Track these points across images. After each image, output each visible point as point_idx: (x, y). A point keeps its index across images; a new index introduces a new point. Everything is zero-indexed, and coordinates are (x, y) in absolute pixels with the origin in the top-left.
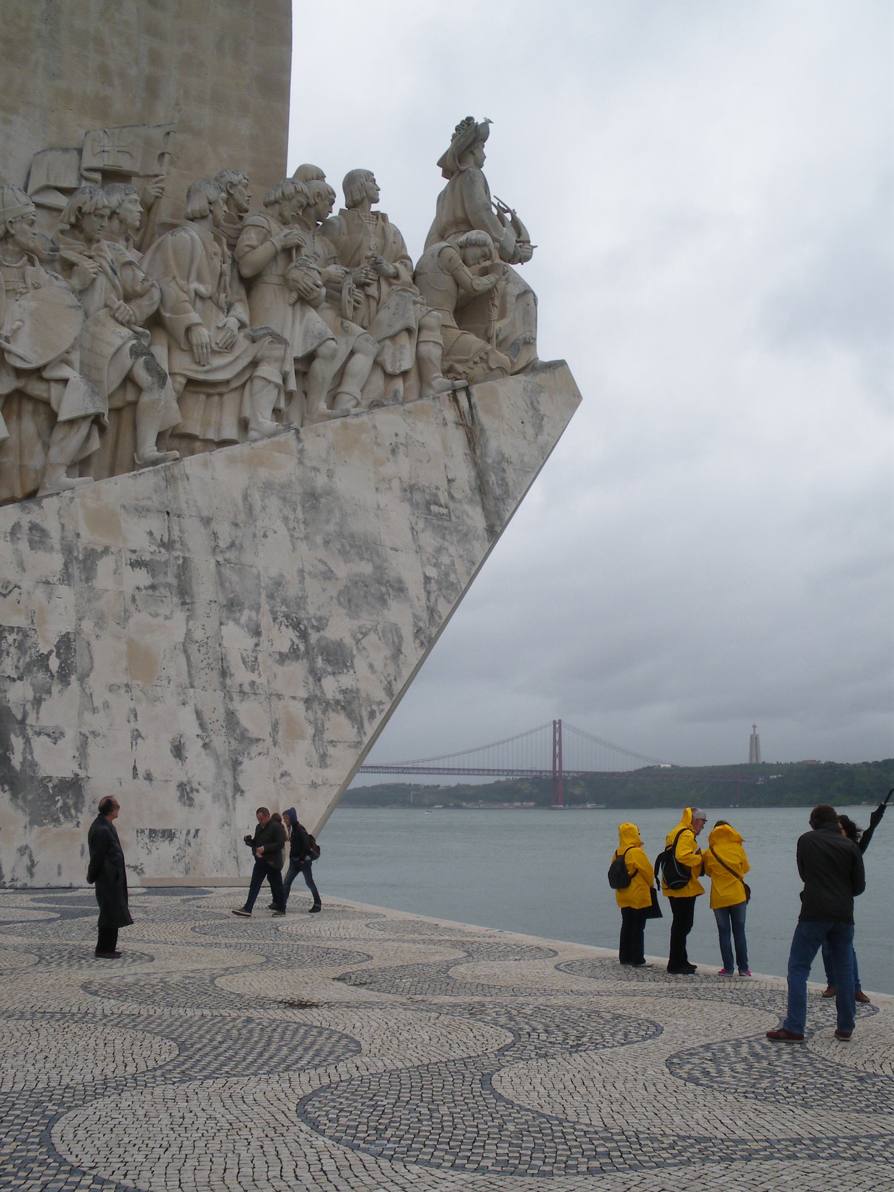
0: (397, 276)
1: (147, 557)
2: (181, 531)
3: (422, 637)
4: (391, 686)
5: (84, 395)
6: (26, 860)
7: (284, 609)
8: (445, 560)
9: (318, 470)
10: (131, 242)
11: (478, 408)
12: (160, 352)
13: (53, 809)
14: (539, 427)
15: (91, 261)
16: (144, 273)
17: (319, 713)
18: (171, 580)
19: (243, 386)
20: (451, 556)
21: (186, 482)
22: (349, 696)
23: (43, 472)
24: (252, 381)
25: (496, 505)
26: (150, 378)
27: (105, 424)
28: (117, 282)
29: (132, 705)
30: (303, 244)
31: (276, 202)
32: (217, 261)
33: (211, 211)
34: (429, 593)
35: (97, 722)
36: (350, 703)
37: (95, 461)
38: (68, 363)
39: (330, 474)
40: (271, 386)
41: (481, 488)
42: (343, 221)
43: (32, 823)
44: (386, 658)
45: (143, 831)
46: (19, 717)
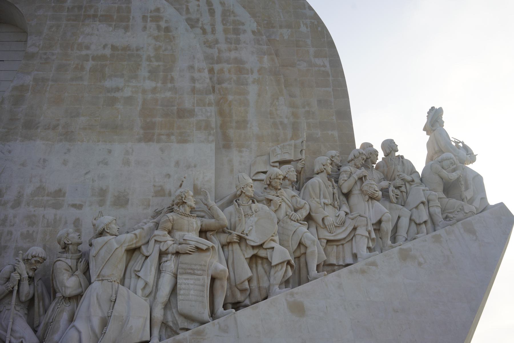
10: (294, 187)
12: (313, 229)
15: (278, 197)
23: (268, 289)
24: (355, 236)
28: (290, 204)
30: (367, 175)
31: (352, 160)
32: (331, 189)
33: (324, 168)
37: (291, 281)
38: (273, 240)
40: (364, 237)
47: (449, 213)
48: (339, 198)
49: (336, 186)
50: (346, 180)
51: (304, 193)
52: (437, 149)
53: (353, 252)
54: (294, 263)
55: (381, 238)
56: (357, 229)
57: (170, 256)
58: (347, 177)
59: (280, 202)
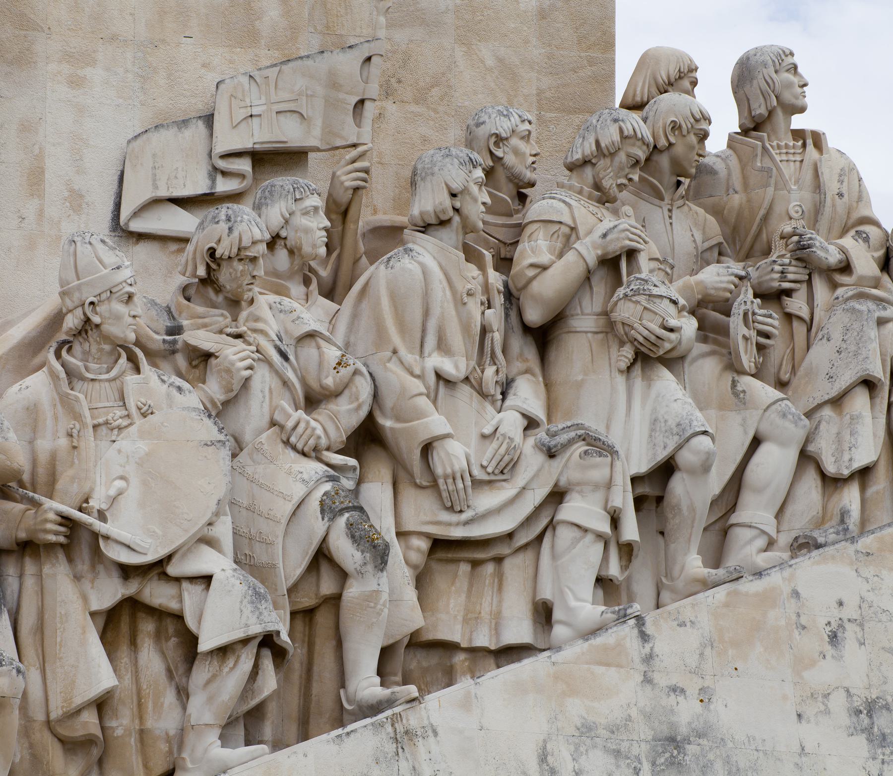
0: (846, 268)
5: (241, 602)
9: (683, 691)
10: (314, 286)
15: (238, 342)
16: (339, 348)
19: (540, 538)
21: (432, 739)
24: (554, 529)
26: (358, 555)
27: (284, 645)
28: (291, 375)
30: (641, 247)
32: (474, 308)
40: (590, 537)
42: (734, 162)
48: (504, 351)
49: (499, 292)
50: (545, 268)
51: (355, 316)
53: (538, 598)
54: (289, 641)
55: (662, 533)
56: (567, 498)
58: (551, 250)
59: (250, 368)
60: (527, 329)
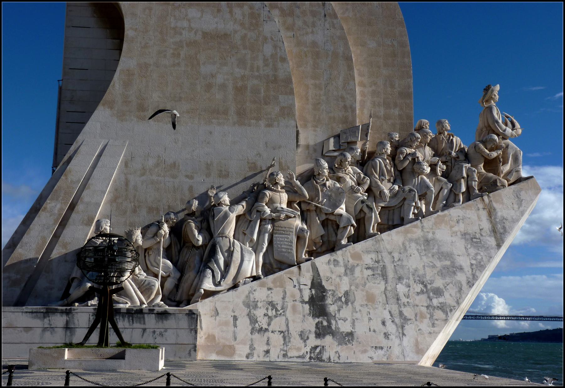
1: (371, 266)
2: (382, 257)
3: (470, 284)
4: (458, 301)
6: (337, 355)
7: (418, 278)
8: (479, 257)
11: (493, 202)
13: (345, 341)
14: (520, 205)
17: (432, 310)
18: (379, 272)
20: (481, 256)
22: (442, 305)
25: (501, 236)
28: (355, 180)
29: (368, 310)
32: (389, 167)
34: (472, 269)
35: (358, 315)
36: (443, 307)
39: (434, 233)
41: (494, 231)
43: (339, 345)
44: (456, 292)
45: (373, 347)
46: (334, 315)
47: (485, 185)
52: (486, 124)
57: (268, 221)
60: (398, 170)
